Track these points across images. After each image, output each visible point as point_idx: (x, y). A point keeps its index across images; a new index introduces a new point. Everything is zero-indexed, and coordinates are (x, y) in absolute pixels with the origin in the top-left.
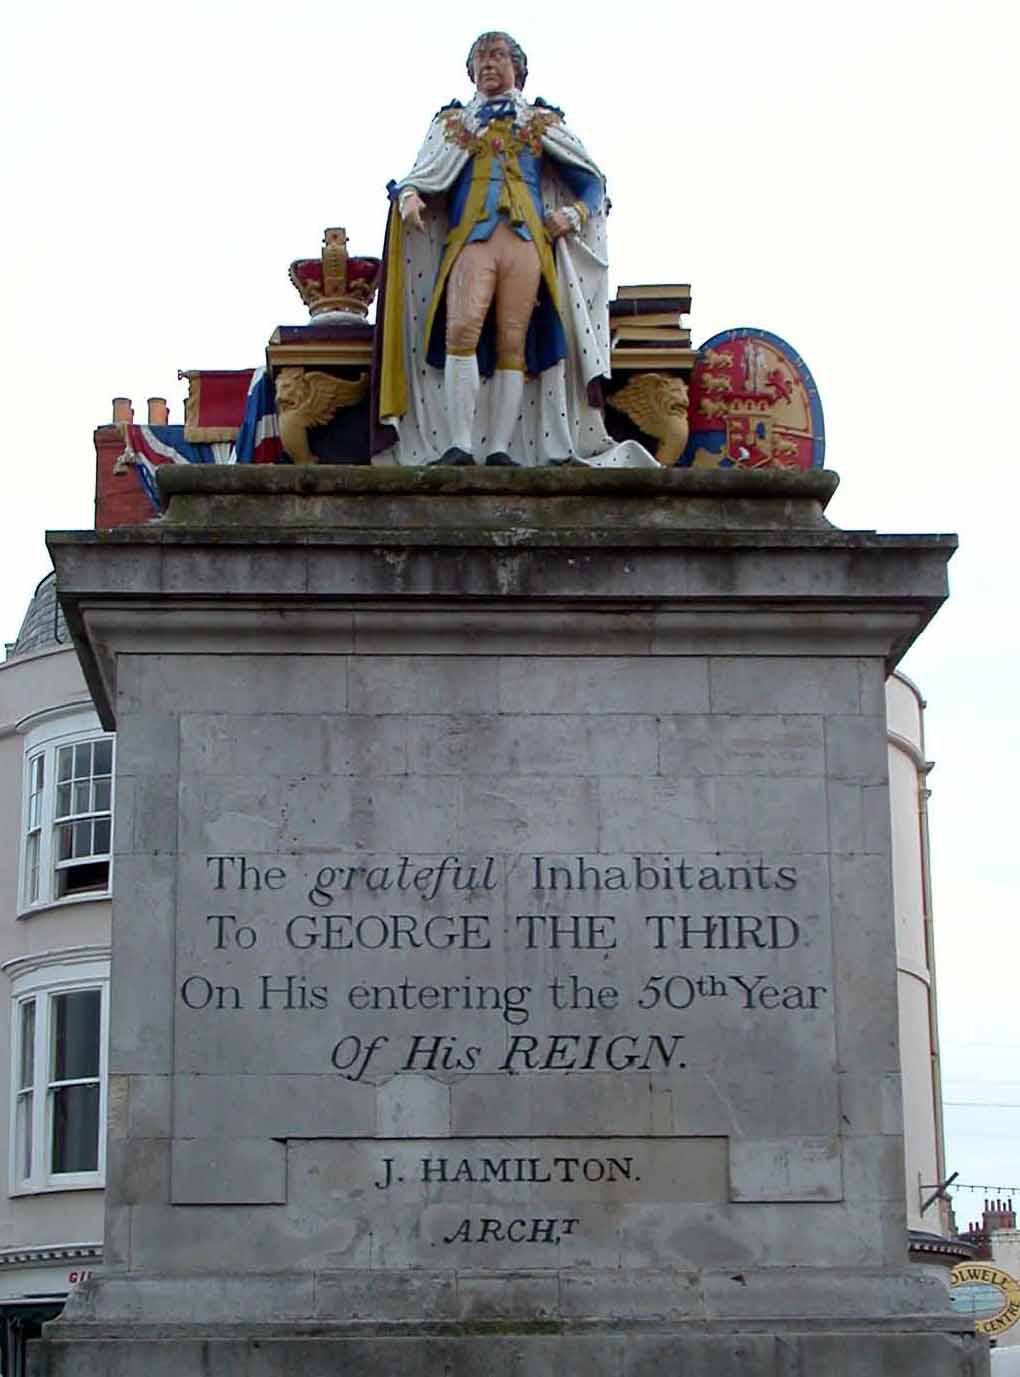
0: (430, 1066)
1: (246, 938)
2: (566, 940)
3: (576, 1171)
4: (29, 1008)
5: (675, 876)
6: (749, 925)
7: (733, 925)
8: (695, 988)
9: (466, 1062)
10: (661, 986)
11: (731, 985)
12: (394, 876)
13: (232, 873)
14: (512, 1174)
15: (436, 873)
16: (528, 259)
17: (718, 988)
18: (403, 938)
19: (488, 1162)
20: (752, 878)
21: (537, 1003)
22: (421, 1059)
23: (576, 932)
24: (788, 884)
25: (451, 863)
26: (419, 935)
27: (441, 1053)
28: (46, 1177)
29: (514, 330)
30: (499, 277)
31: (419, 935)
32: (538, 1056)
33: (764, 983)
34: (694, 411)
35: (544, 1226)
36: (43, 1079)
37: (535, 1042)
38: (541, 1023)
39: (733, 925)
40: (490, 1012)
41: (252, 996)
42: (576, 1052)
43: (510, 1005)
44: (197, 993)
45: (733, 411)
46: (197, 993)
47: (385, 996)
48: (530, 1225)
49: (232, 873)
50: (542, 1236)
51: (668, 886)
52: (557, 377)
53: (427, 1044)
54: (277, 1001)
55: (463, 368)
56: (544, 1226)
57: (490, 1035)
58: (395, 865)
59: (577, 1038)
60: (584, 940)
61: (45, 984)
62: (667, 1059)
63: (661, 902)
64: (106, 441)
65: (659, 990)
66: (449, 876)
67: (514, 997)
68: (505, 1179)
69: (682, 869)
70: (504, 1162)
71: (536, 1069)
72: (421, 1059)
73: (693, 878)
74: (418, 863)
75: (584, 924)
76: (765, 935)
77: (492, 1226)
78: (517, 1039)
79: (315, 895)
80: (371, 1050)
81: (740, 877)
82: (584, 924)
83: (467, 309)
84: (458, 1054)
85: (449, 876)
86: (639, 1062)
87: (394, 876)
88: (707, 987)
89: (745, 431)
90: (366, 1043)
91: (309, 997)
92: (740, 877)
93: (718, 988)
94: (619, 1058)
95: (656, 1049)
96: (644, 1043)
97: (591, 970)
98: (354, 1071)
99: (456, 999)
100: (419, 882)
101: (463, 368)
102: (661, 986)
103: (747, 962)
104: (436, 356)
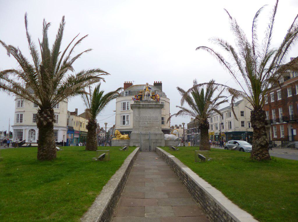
4: (121, 116)
16: (148, 92)
28: (122, 125)
29: (148, 95)
30: (147, 93)
34: (155, 98)
36: (122, 120)
38: (149, 122)
52: (149, 97)
55: (146, 96)
57: (146, 123)
61: (122, 115)
64: (124, 84)
83: (146, 94)
97: (150, 121)
101: (146, 96)
104: (145, 96)
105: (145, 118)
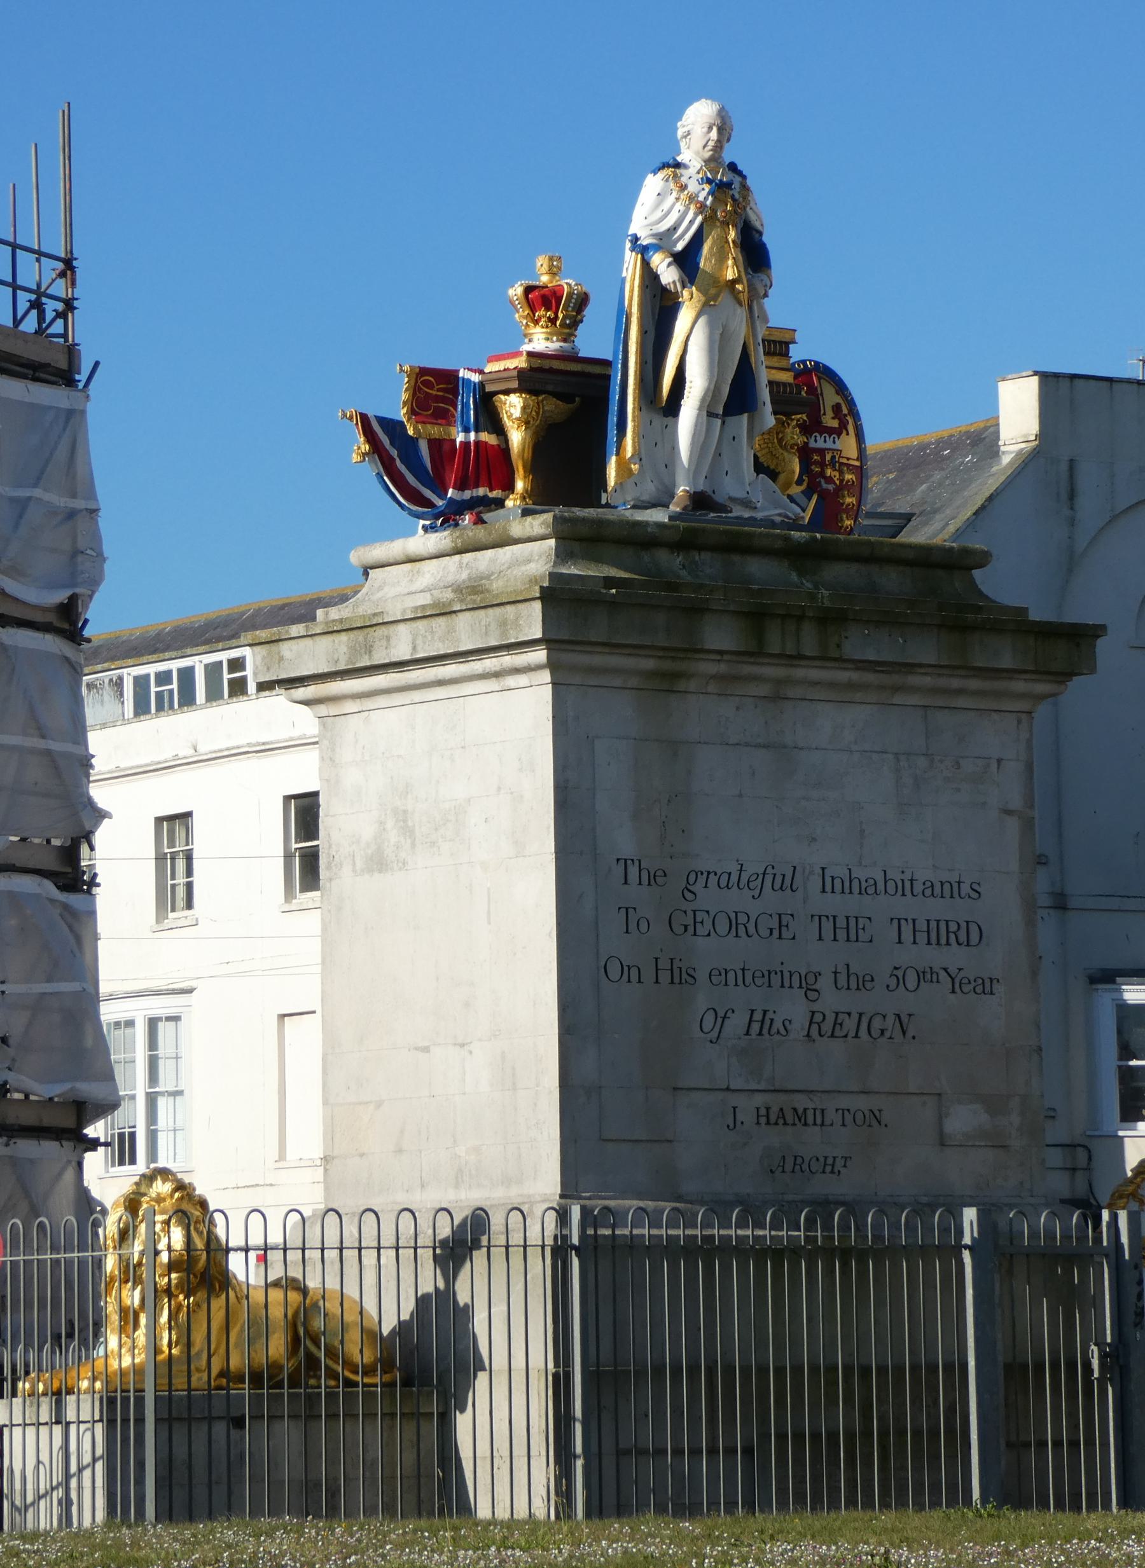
0: (760, 1034)
1: (644, 926)
2: (842, 934)
3: (849, 1118)
5: (908, 884)
6: (953, 927)
7: (943, 926)
8: (921, 976)
9: (783, 1031)
10: (900, 973)
11: (943, 974)
12: (734, 878)
13: (633, 871)
14: (810, 1120)
15: (761, 877)
17: (935, 977)
18: (741, 929)
19: (795, 1110)
20: (951, 890)
21: (825, 983)
22: (756, 1027)
23: (848, 928)
24: (975, 895)
25: (769, 870)
26: (752, 930)
27: (767, 1022)
31: (752, 930)
32: (827, 1027)
33: (962, 974)
35: (830, 1161)
37: (824, 1015)
38: (831, 1000)
39: (943, 926)
40: (796, 991)
41: (648, 975)
42: (850, 1024)
43: (810, 989)
44: (614, 971)
45: (812, 444)
46: (614, 971)
47: (731, 975)
48: (822, 1160)
49: (633, 871)
50: (828, 1169)
51: (903, 895)
53: (758, 1016)
54: (665, 977)
56: (830, 1161)
58: (734, 868)
59: (849, 1014)
60: (853, 937)
62: (904, 1033)
63: (905, 907)
65: (898, 976)
66: (769, 879)
67: (811, 979)
68: (806, 1124)
69: (912, 880)
70: (805, 1110)
71: (825, 1037)
72: (756, 1027)
73: (918, 888)
74: (751, 869)
75: (852, 922)
76: (963, 937)
77: (799, 1161)
78: (813, 1013)
79: (687, 893)
80: (724, 1018)
81: (947, 887)
82: (852, 922)
84: (778, 1024)
85: (769, 879)
86: (887, 1034)
87: (734, 878)
88: (928, 976)
89: (822, 464)
90: (721, 1014)
91: (684, 976)
92: (947, 887)
93: (935, 977)
94: (875, 1033)
95: (898, 1025)
96: (891, 1019)
98: (715, 1034)
99: (776, 980)
100: (751, 884)
102: (900, 973)
103: (954, 957)
105: (772, 901)
